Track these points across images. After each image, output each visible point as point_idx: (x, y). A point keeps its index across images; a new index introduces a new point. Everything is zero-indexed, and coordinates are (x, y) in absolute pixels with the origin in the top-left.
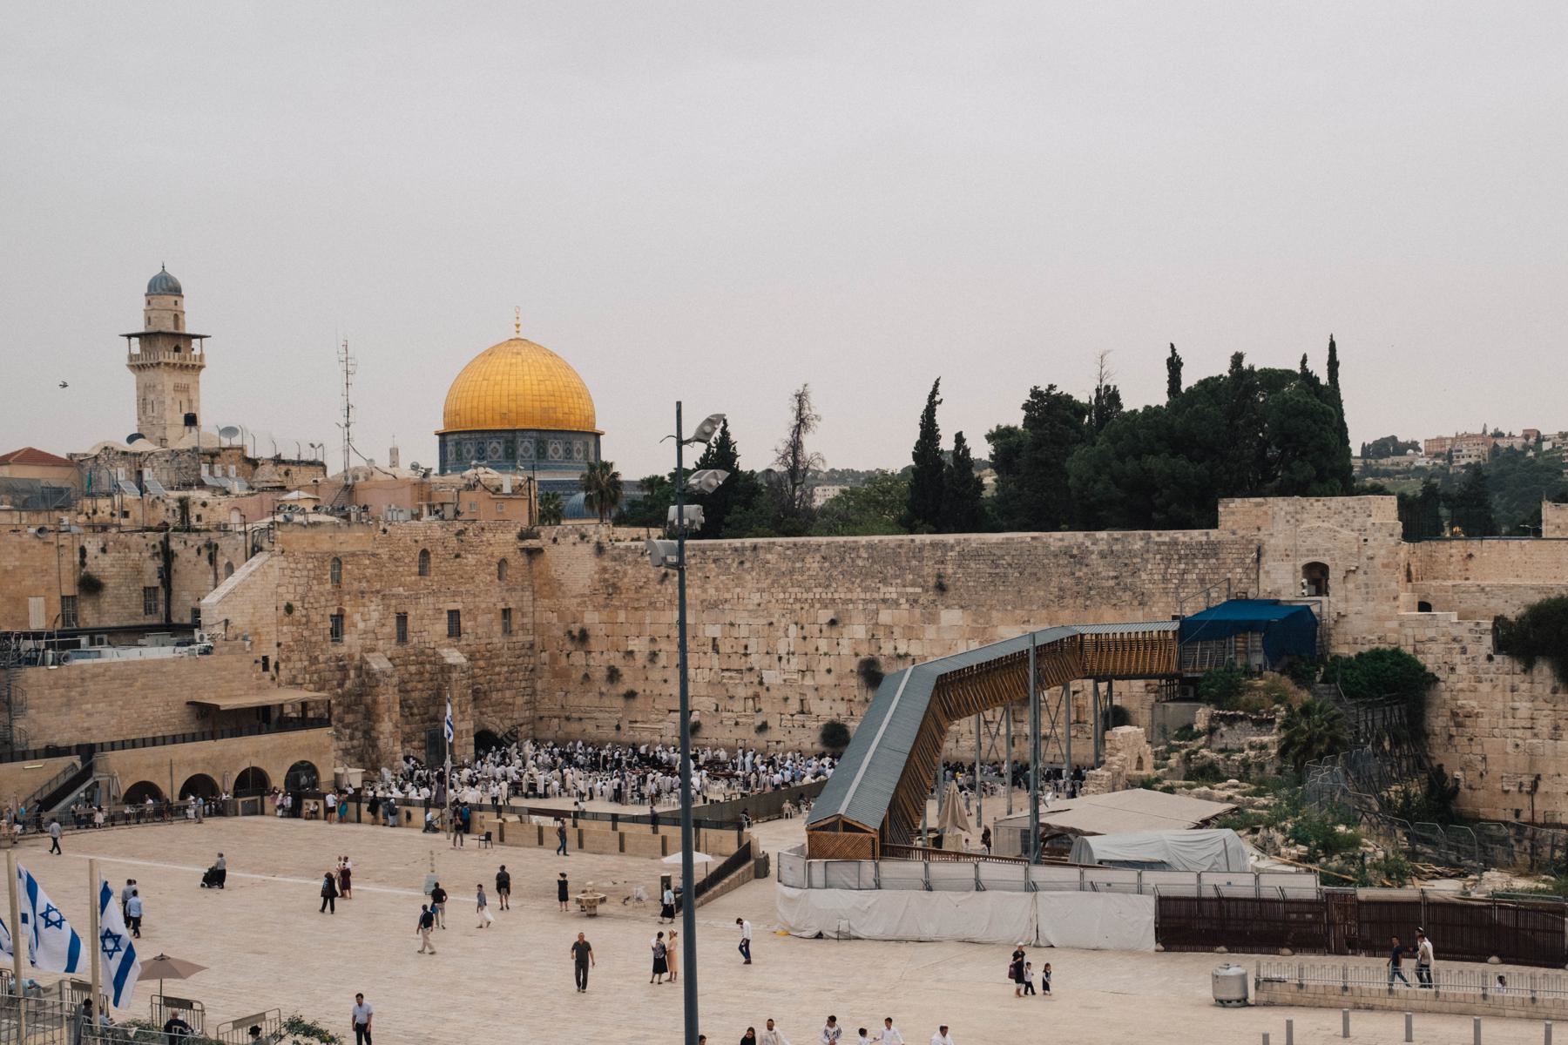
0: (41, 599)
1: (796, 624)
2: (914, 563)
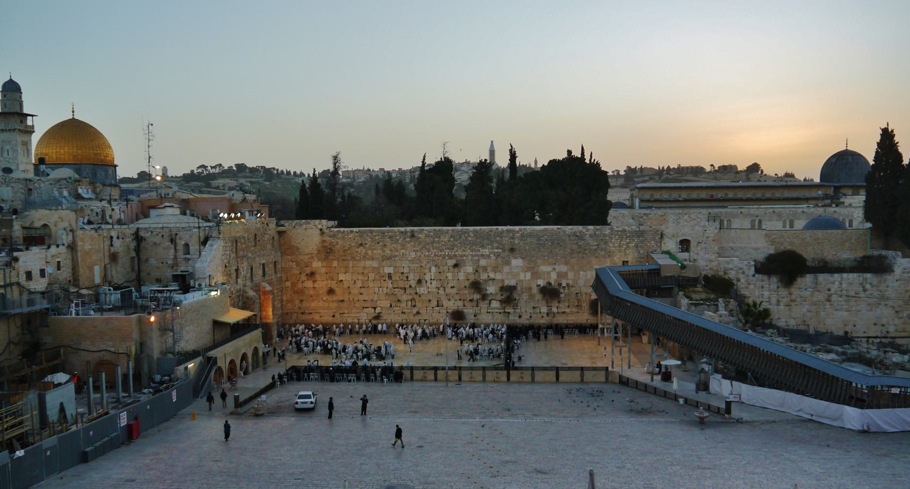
2: (498, 239)
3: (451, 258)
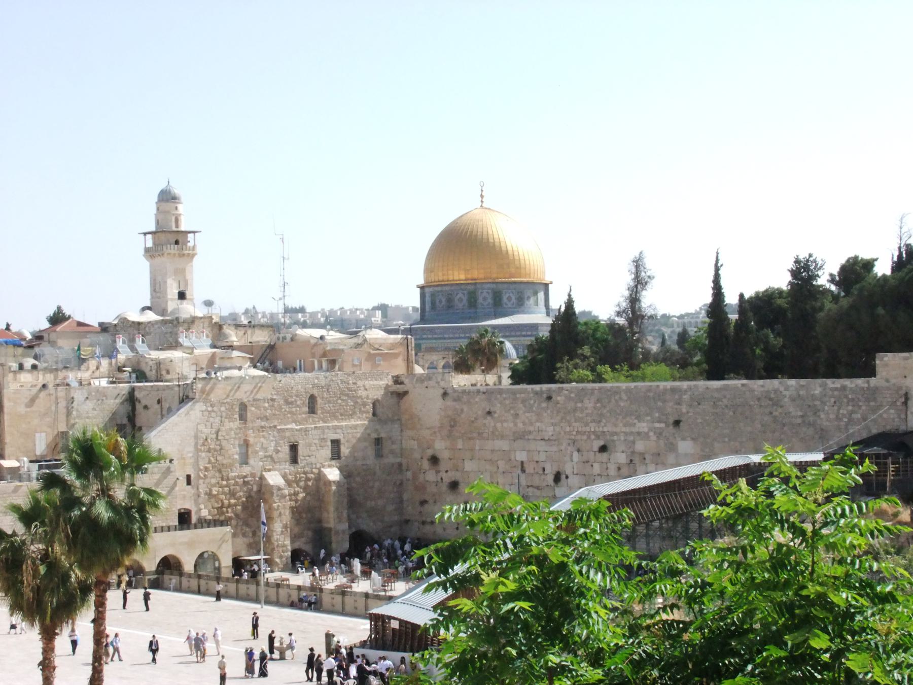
0: (43, 435)
1: (579, 451)
2: (660, 404)
3: (598, 437)
